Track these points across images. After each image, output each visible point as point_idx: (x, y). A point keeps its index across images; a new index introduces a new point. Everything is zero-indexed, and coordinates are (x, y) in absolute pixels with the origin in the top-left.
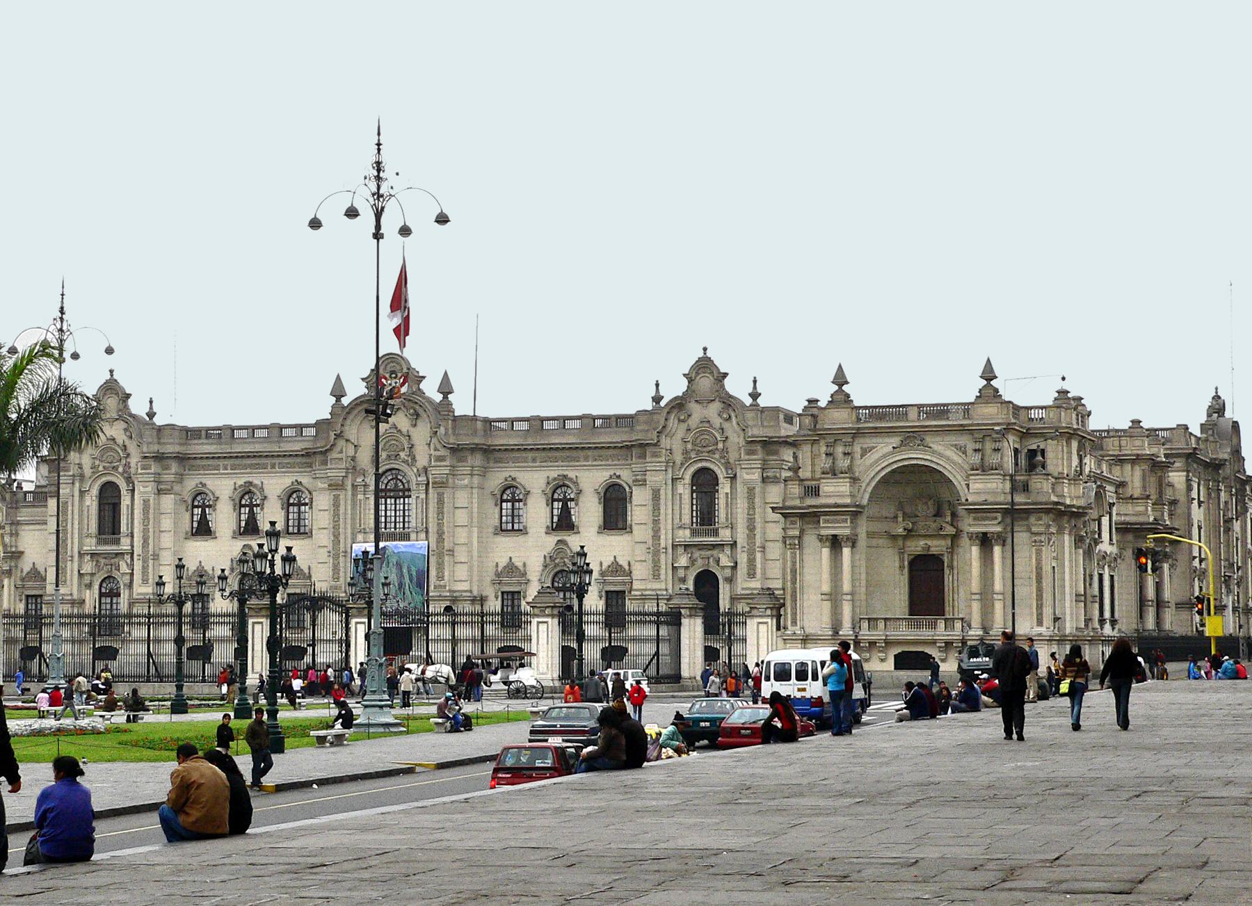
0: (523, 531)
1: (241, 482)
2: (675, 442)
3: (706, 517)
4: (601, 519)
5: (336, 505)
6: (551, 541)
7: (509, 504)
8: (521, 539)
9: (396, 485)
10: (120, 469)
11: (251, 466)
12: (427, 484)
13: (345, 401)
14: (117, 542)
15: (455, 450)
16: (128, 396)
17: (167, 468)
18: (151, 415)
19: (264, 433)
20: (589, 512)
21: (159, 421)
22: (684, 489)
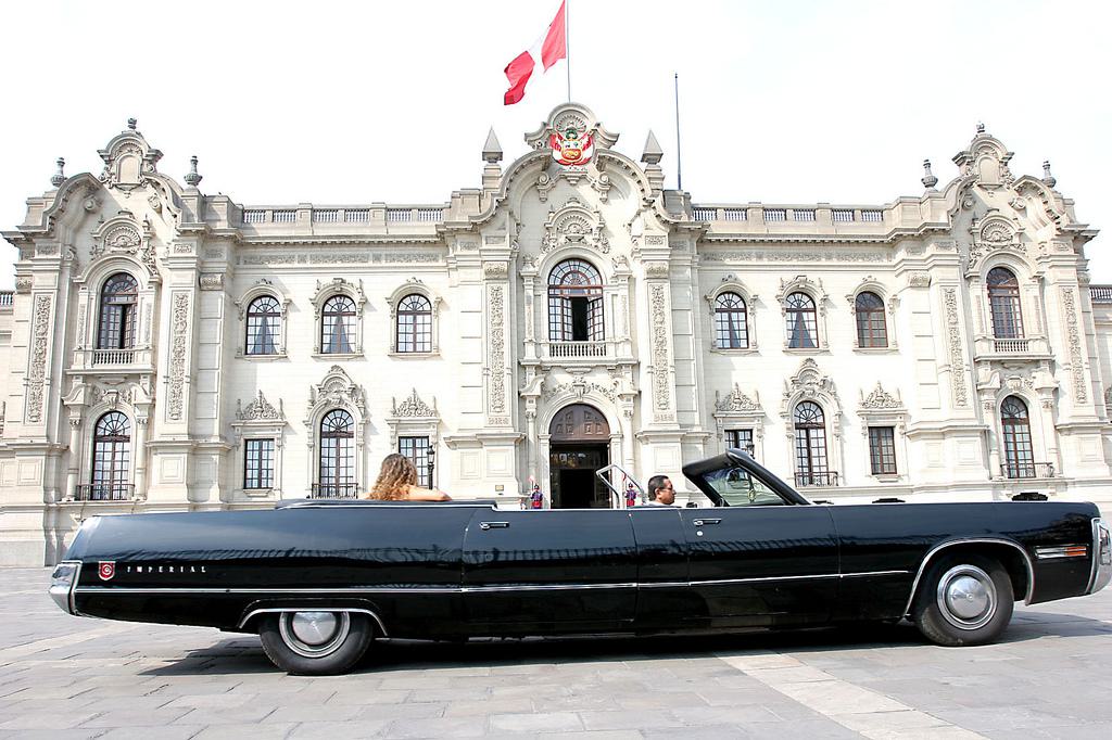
1: (327, 280)
2: (961, 235)
3: (1005, 326)
5: (497, 300)
7: (725, 315)
10: (140, 254)
11: (343, 259)
13: (505, 164)
14: (129, 358)
15: (675, 229)
16: (157, 155)
17: (214, 254)
18: (195, 180)
20: (838, 324)
21: (205, 188)
22: (979, 291)
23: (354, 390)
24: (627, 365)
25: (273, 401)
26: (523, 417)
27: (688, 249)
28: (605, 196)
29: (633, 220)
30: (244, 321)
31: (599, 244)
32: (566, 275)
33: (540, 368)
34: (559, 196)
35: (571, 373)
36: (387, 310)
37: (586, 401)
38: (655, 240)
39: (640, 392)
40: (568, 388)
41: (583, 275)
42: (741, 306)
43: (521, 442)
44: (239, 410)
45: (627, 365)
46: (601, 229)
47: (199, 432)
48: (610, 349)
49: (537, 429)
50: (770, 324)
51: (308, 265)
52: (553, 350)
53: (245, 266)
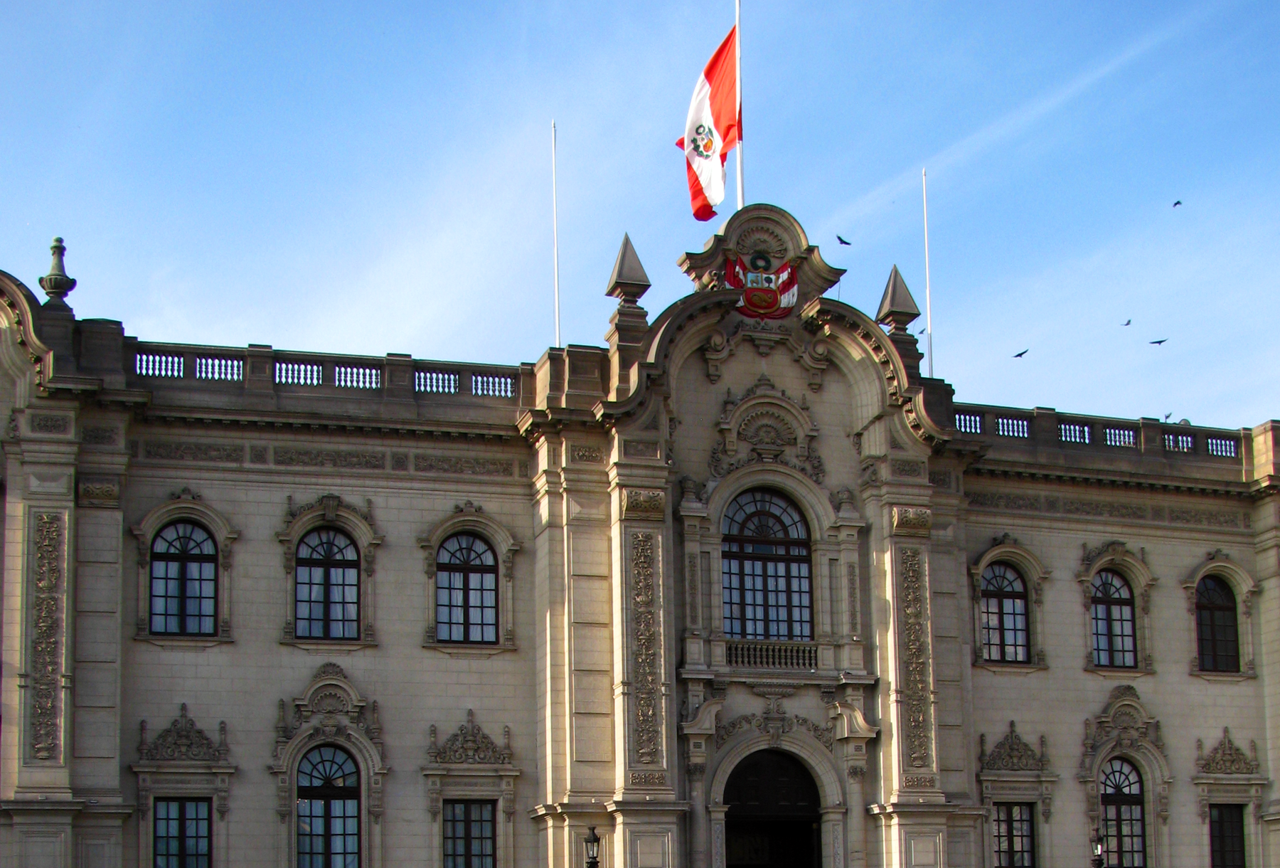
0: (1033, 659)
1: (306, 495)
4: (1194, 646)
6: (1098, 688)
7: (993, 603)
8: (1031, 680)
9: (762, 528)
11: (337, 459)
12: (864, 532)
19: (368, 380)
23: (366, 712)
24: (856, 687)
25: (207, 723)
26: (689, 772)
27: (953, 485)
28: (817, 381)
29: (866, 428)
30: (148, 568)
31: (808, 467)
32: (749, 517)
33: (714, 688)
34: (740, 370)
35: (762, 695)
36: (418, 560)
37: (786, 746)
38: (905, 468)
39: (878, 733)
40: (754, 723)
41: (778, 519)
42: (1018, 586)
43: (686, 821)
44: (142, 742)
45: (856, 687)
46: (812, 438)
47: (89, 782)
48: (826, 656)
49: (708, 793)
50: (1064, 619)
51: (273, 467)
52: (732, 654)
53: (148, 461)
